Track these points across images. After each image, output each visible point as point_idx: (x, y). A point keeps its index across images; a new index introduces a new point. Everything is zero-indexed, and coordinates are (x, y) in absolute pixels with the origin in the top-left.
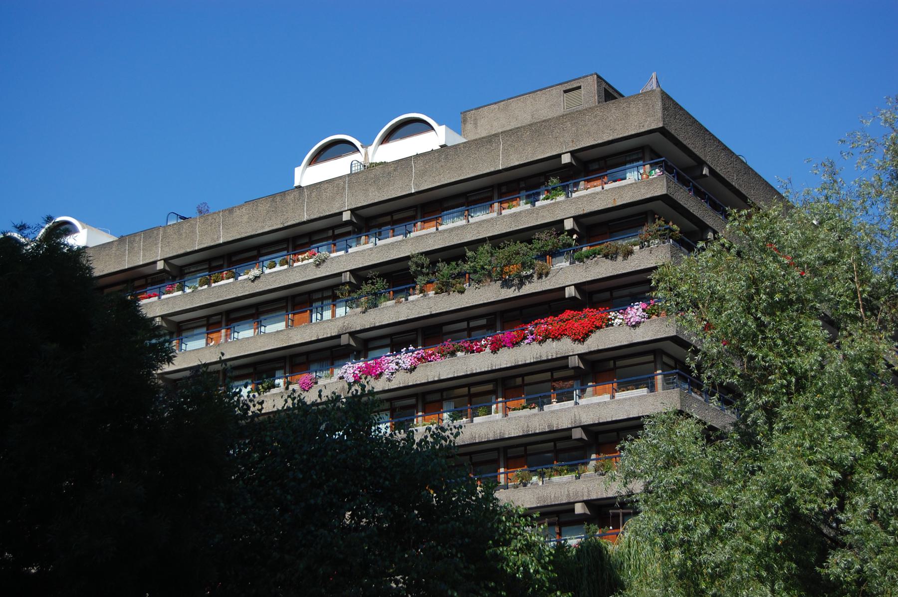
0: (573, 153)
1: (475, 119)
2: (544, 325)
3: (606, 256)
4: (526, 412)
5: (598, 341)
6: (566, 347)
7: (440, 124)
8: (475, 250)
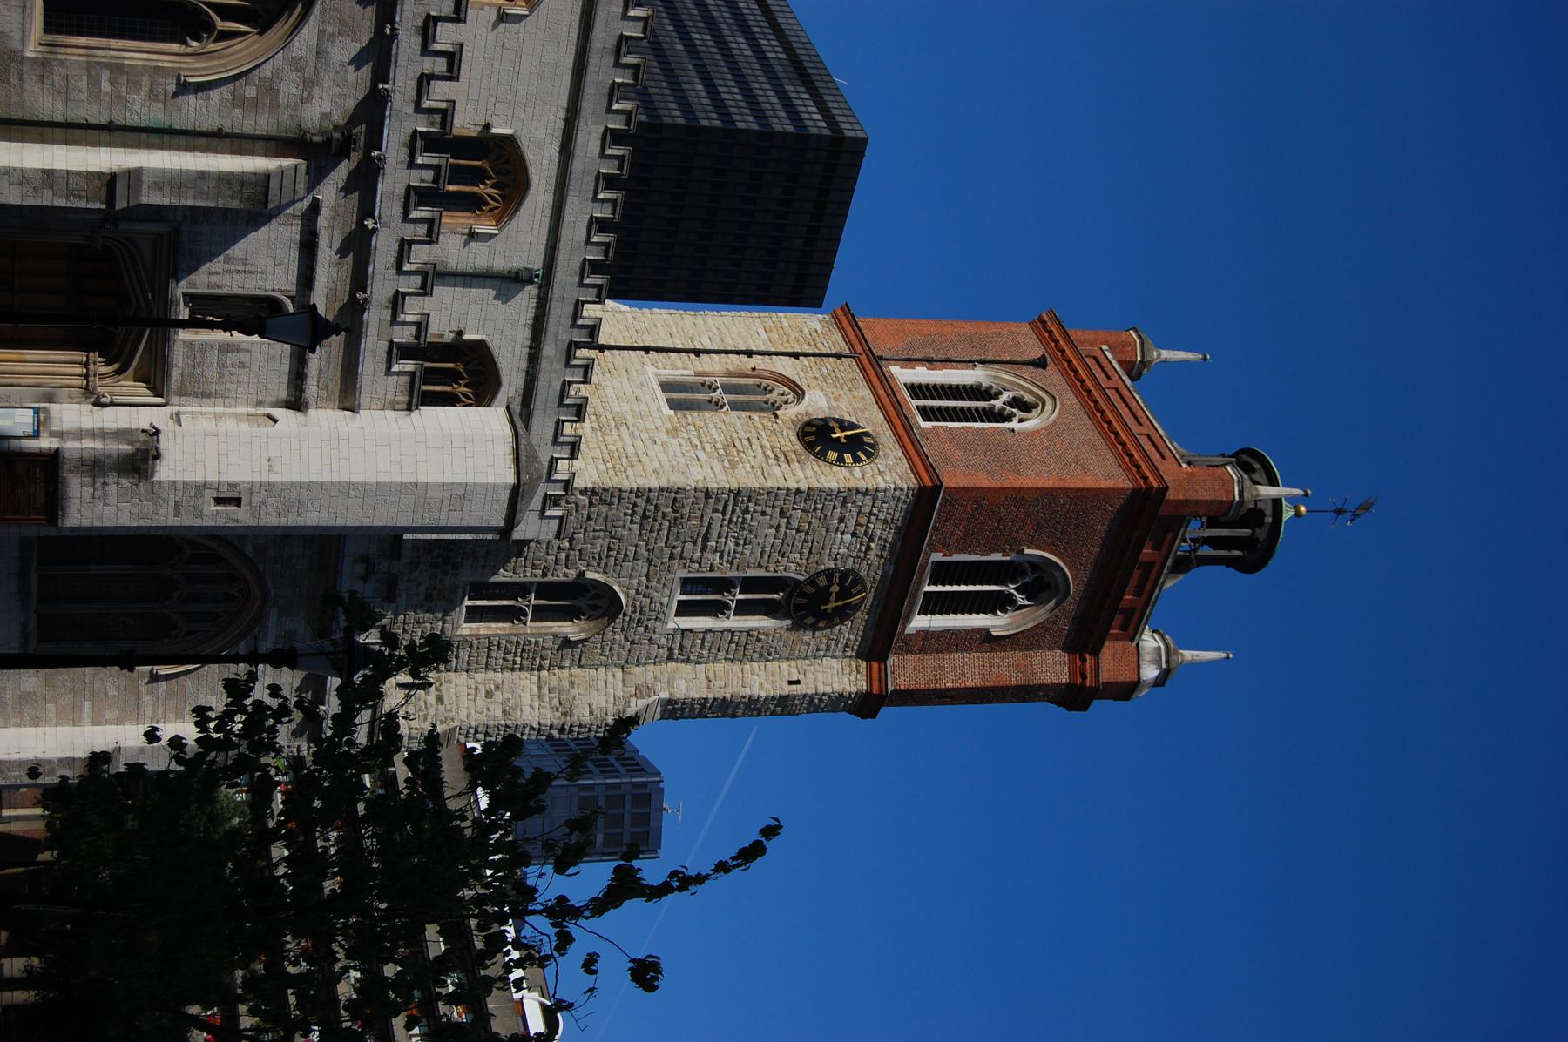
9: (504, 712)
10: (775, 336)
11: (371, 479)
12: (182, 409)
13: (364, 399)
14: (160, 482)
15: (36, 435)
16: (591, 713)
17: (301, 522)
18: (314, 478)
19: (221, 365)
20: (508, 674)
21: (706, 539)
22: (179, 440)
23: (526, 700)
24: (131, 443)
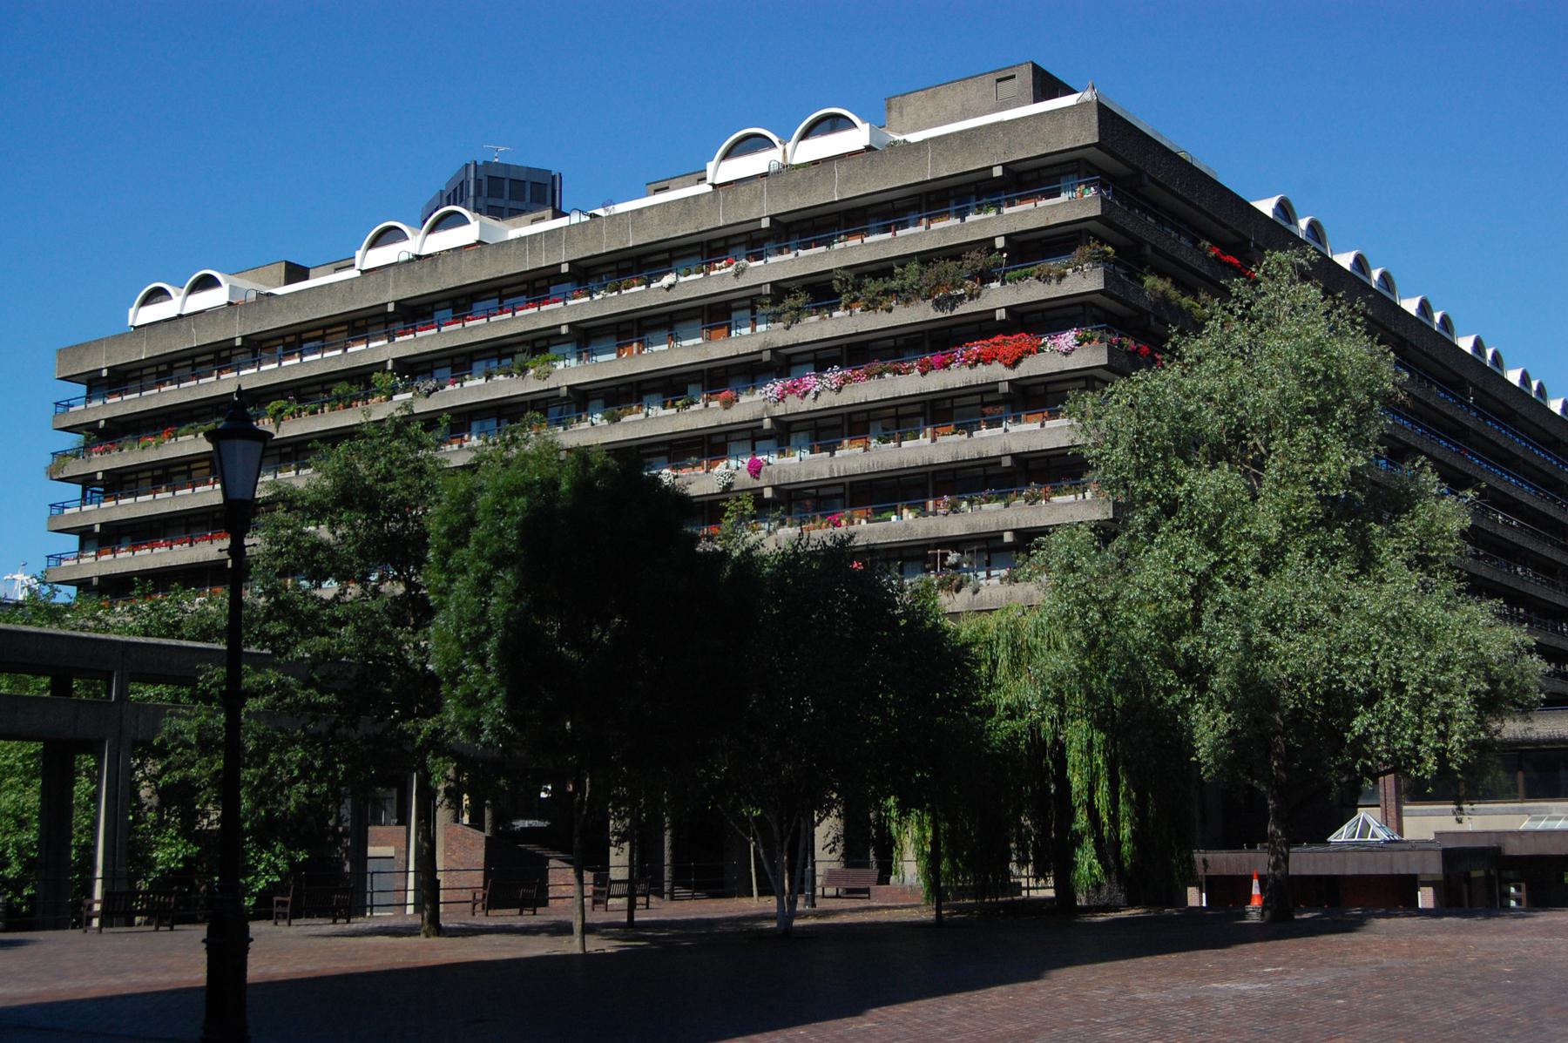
0: (1004, 165)
1: (901, 108)
2: (976, 348)
3: (1038, 278)
4: (956, 437)
5: (1032, 367)
6: (997, 372)
7: (864, 121)
8: (903, 266)
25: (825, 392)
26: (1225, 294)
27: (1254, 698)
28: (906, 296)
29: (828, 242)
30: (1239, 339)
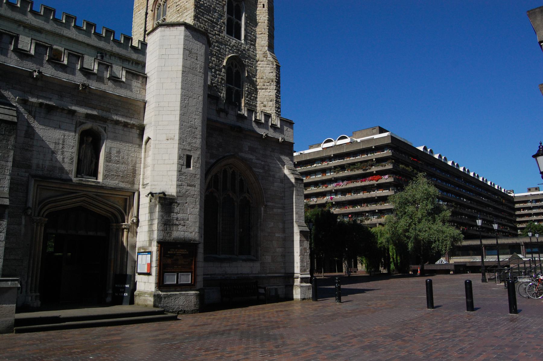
5: (380, 181)
6: (374, 182)
9: (271, 101)
10: (141, 7)
11: (179, 92)
12: (141, 183)
13: (139, 97)
14: (177, 192)
15: (150, 253)
16: (272, 72)
17: (200, 128)
18: (178, 118)
19: (118, 162)
20: (258, 99)
21: (212, 22)
22: (156, 183)
23: (267, 94)
24: (156, 205)
25: (344, 185)
26: (412, 179)
27: (417, 241)
28: (358, 169)
29: (344, 159)
30: (414, 187)
